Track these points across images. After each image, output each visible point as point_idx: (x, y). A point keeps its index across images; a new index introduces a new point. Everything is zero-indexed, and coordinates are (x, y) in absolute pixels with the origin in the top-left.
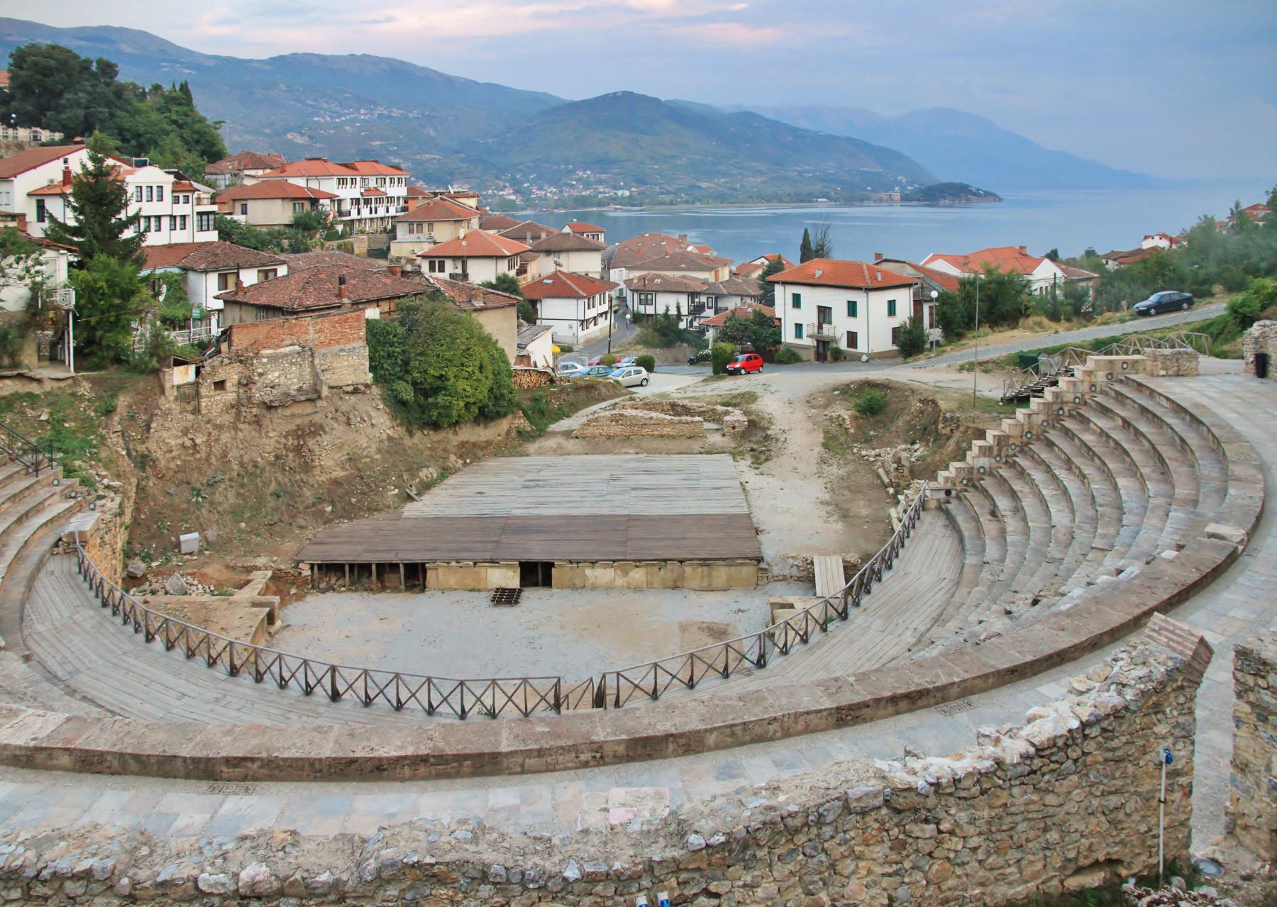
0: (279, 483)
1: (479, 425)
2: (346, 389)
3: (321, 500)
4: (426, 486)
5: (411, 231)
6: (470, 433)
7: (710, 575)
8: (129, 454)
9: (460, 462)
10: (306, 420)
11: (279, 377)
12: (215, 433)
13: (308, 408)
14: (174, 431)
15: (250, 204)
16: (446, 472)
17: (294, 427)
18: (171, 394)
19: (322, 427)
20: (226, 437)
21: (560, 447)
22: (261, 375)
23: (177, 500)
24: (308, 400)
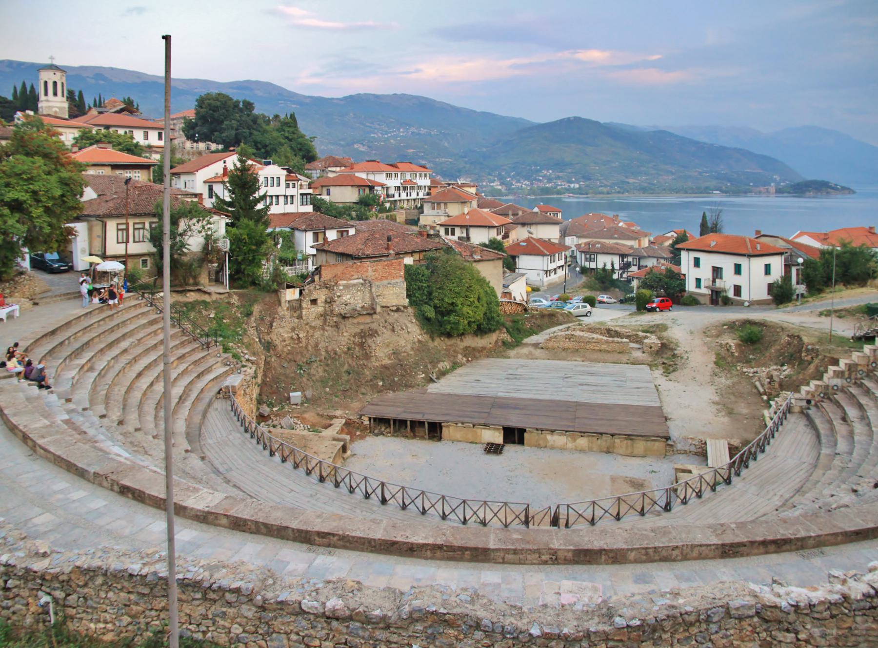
0: (350, 365)
1: (477, 336)
3: (375, 377)
4: (443, 374)
5: (433, 208)
6: (471, 341)
7: (632, 446)
8: (260, 341)
9: (465, 359)
10: (367, 326)
12: (311, 331)
13: (368, 319)
14: (286, 329)
15: (332, 189)
16: (455, 366)
17: (359, 331)
18: (285, 306)
19: (376, 332)
20: (318, 334)
21: (531, 353)
22: (339, 296)
23: (288, 372)
24: (368, 314)
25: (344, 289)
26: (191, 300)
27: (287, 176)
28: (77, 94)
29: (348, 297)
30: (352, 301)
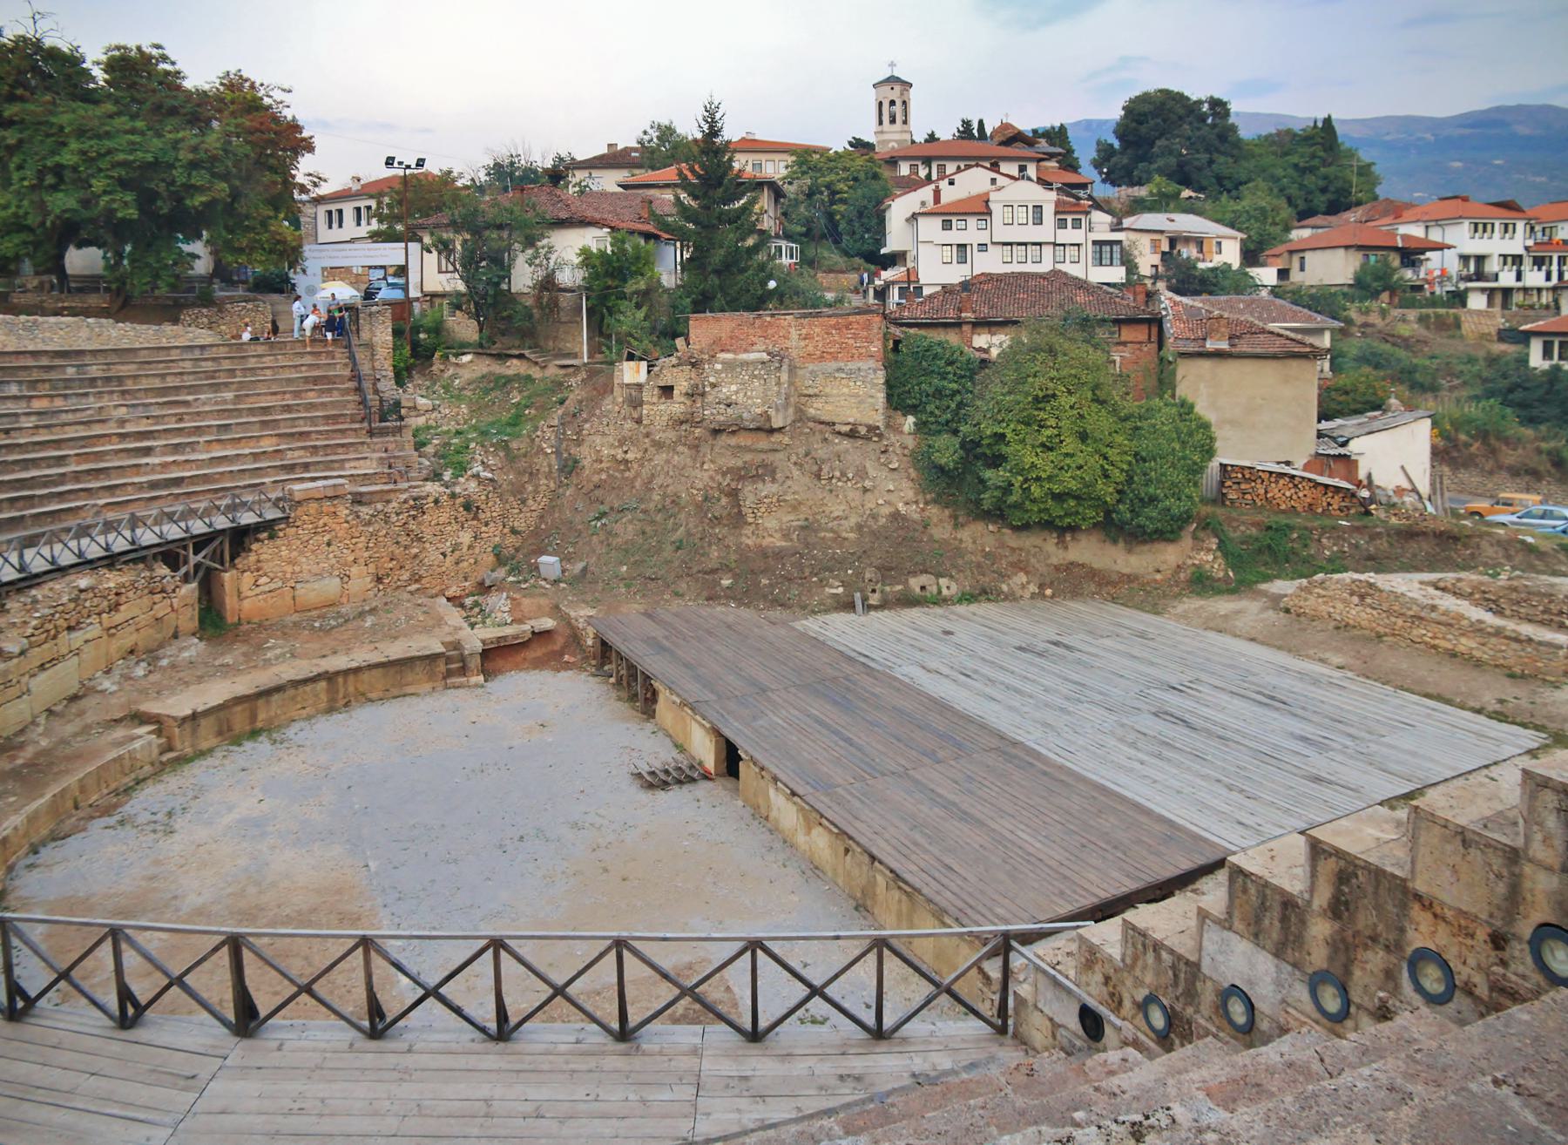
1: (1115, 542)
2: (837, 428)
3: (725, 568)
4: (908, 601)
6: (1088, 551)
8: (558, 453)
10: (759, 458)
11: (737, 392)
14: (611, 439)
15: (1308, 256)
17: (740, 463)
19: (773, 472)
20: (660, 458)
22: (713, 386)
23: (578, 519)
26: (510, 372)
27: (1058, 203)
28: (975, 125)
29: (734, 388)
30: (740, 398)
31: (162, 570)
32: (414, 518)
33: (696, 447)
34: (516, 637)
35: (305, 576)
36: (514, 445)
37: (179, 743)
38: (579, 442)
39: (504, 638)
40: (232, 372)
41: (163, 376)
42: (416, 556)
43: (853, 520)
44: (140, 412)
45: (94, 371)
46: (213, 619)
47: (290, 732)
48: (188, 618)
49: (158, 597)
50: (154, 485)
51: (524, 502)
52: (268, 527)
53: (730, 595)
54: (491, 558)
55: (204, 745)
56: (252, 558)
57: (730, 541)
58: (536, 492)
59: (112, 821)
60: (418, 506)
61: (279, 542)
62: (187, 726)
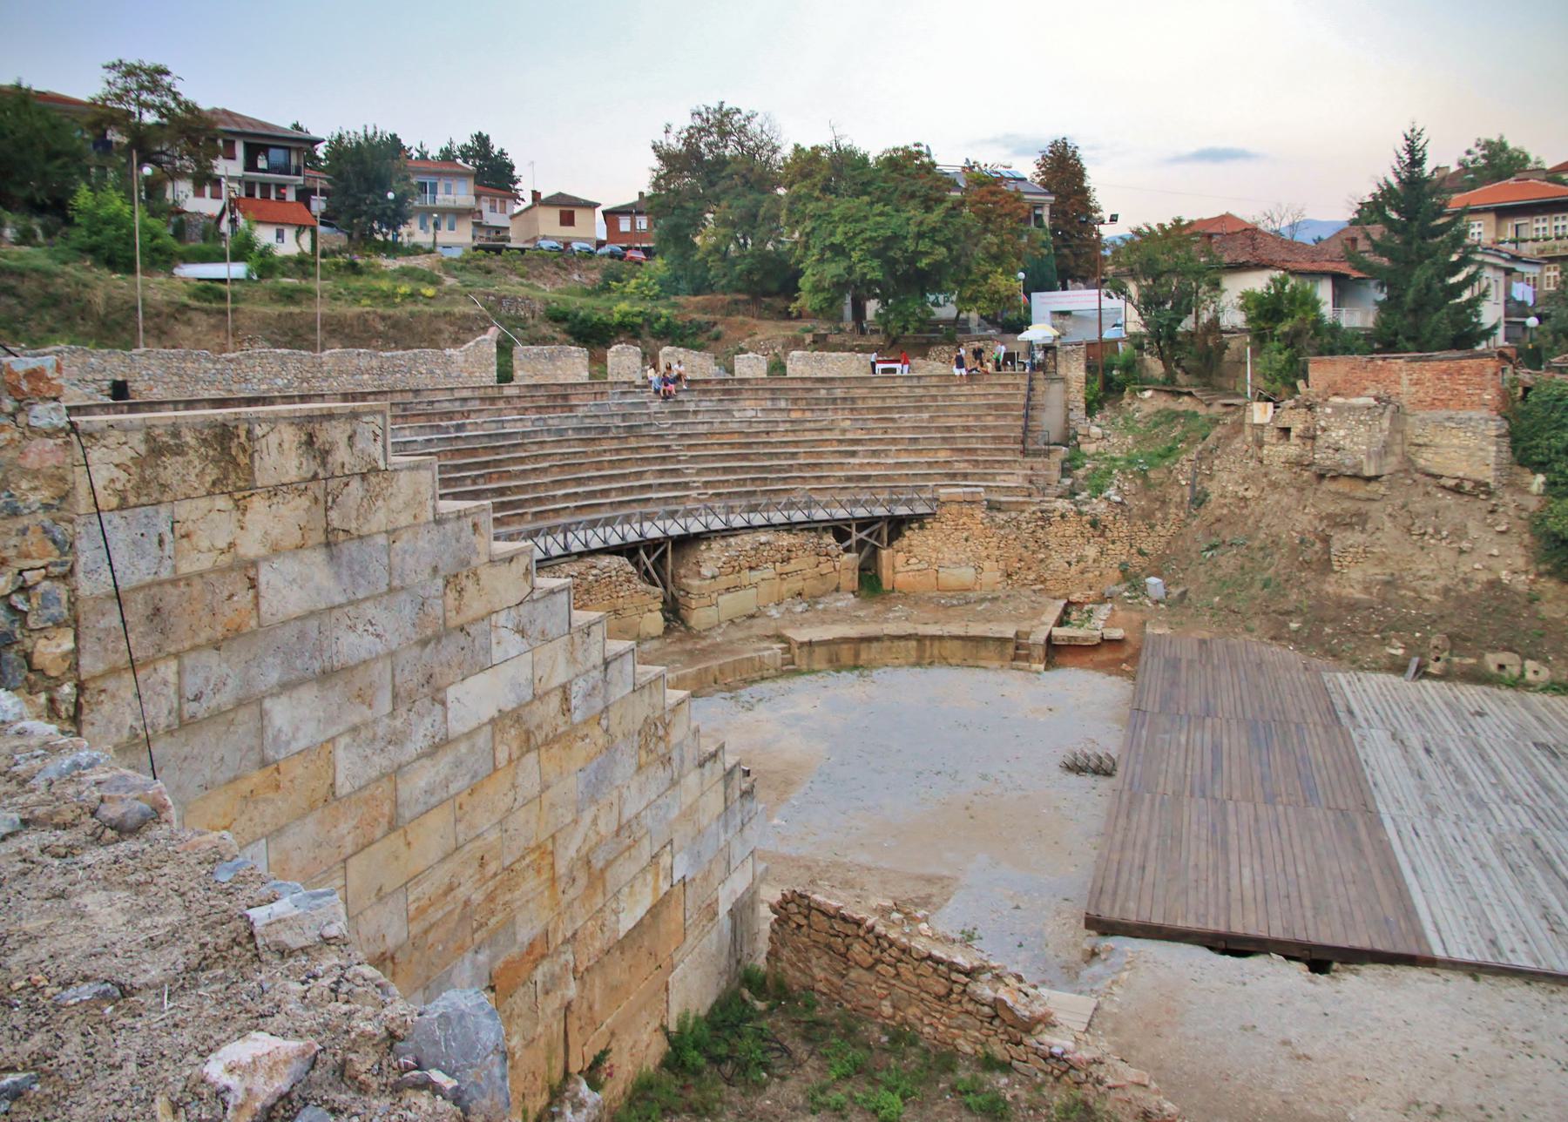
2: (1443, 481)
4: (1477, 677)
8: (1193, 487)
11: (1344, 438)
14: (1236, 476)
20: (1272, 498)
22: (1324, 430)
25: (1333, 414)
29: (1342, 433)
30: (1347, 443)
31: (829, 539)
32: (1043, 528)
33: (1301, 490)
34: (1085, 639)
35: (946, 563)
36: (1152, 475)
37: (796, 661)
38: (1211, 477)
39: (1075, 638)
40: (934, 398)
41: (884, 398)
42: (1042, 561)
43: (1441, 582)
44: (859, 424)
45: (839, 393)
46: (870, 582)
47: (875, 673)
48: (850, 579)
49: (822, 559)
50: (849, 479)
51: (1152, 527)
52: (919, 518)
53: (1297, 640)
54: (1117, 574)
55: (816, 667)
56: (905, 542)
57: (1311, 587)
58: (1165, 519)
59: (728, 695)
60: (1045, 518)
61: (927, 532)
62: (805, 649)
